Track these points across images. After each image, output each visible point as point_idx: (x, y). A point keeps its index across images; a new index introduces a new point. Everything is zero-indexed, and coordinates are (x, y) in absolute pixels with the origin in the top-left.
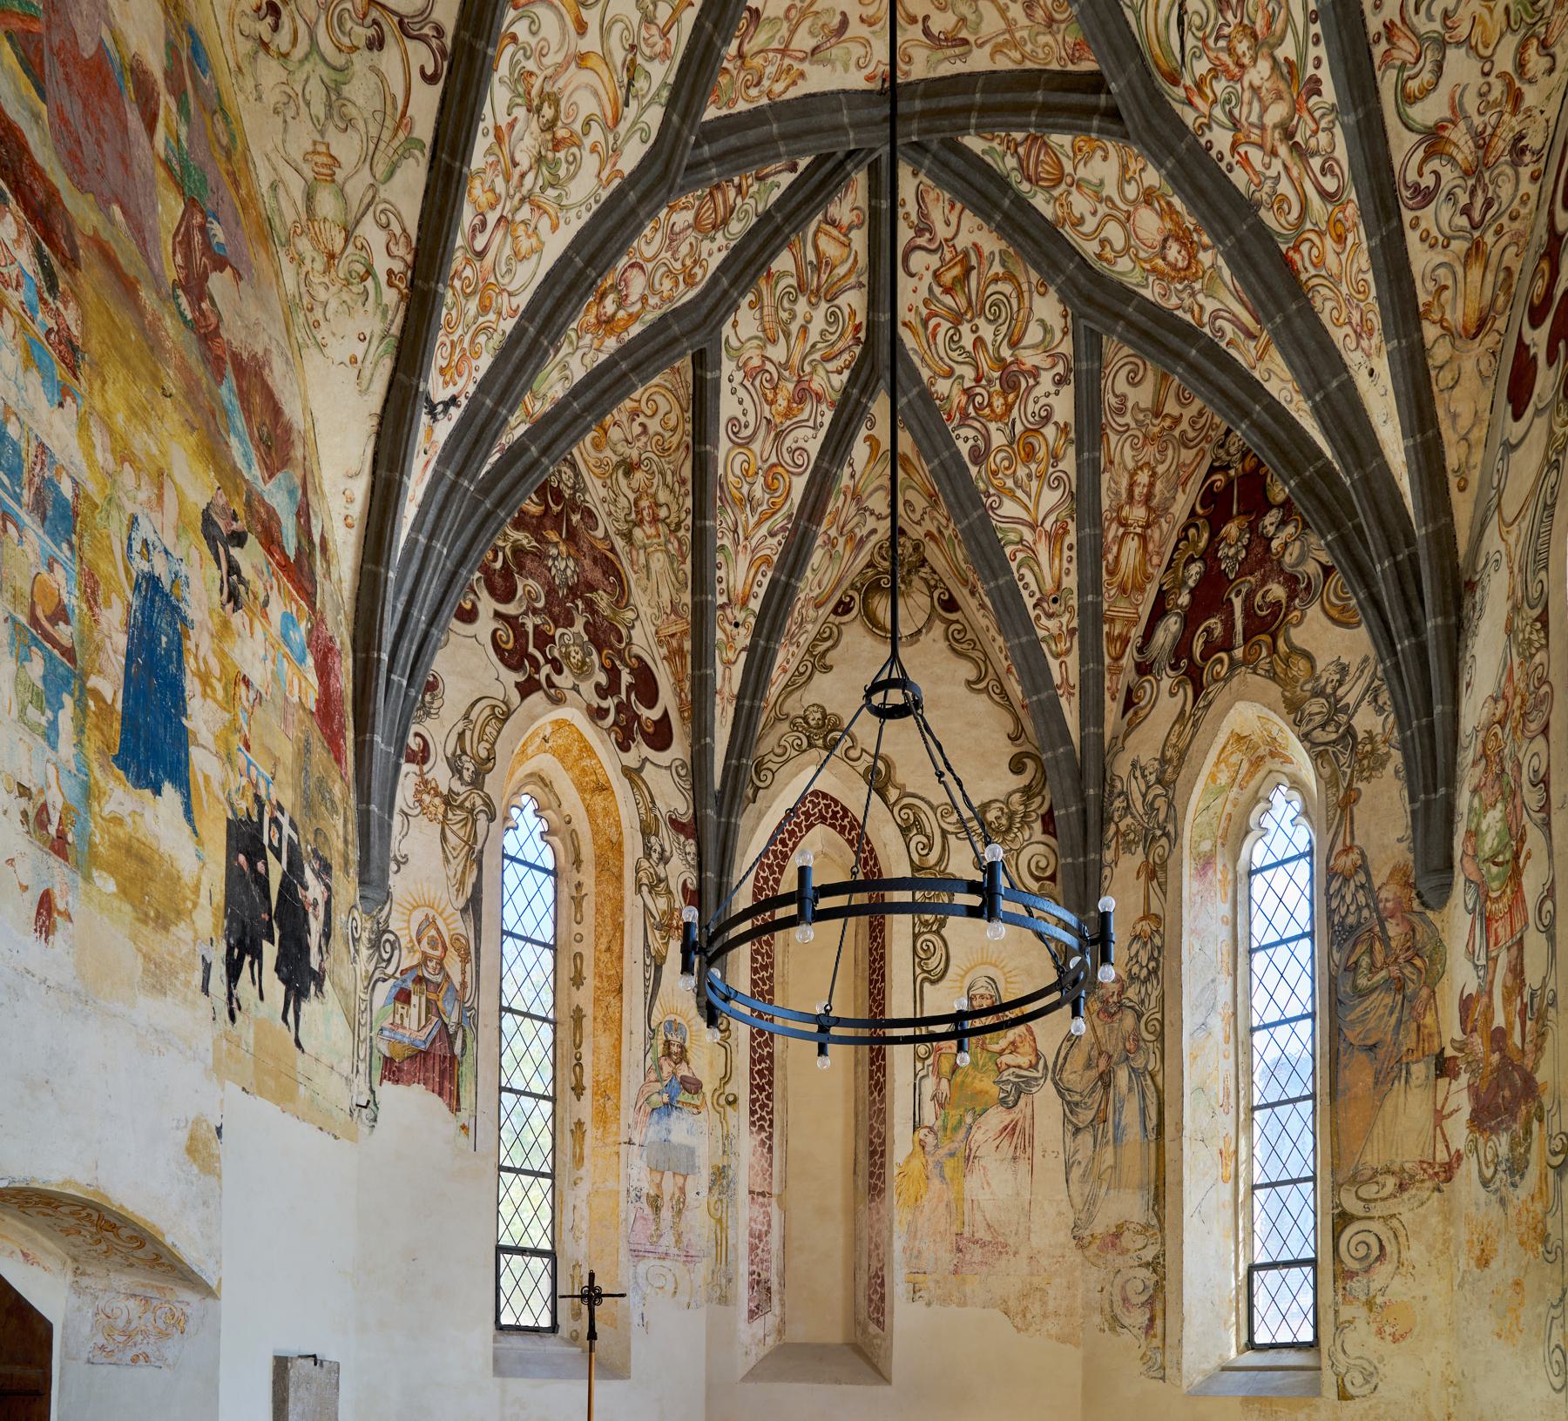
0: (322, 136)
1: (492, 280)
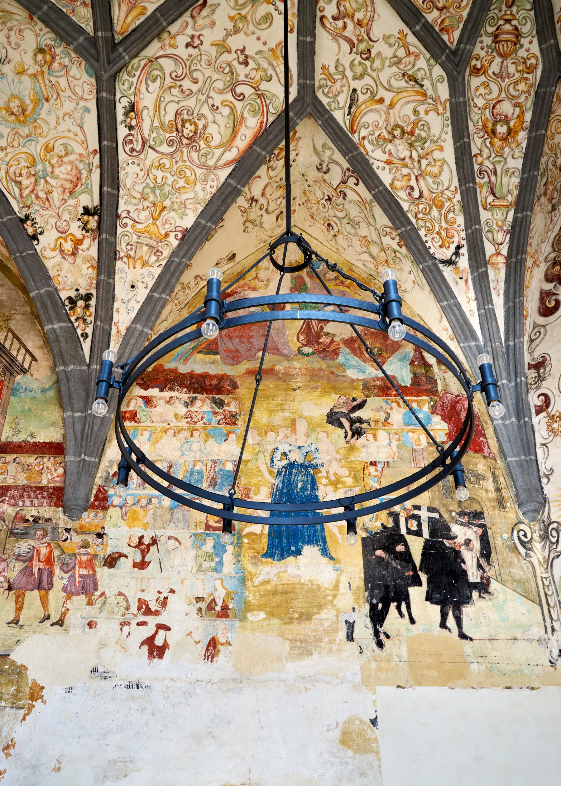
0: (358, 235)
1: (434, 195)
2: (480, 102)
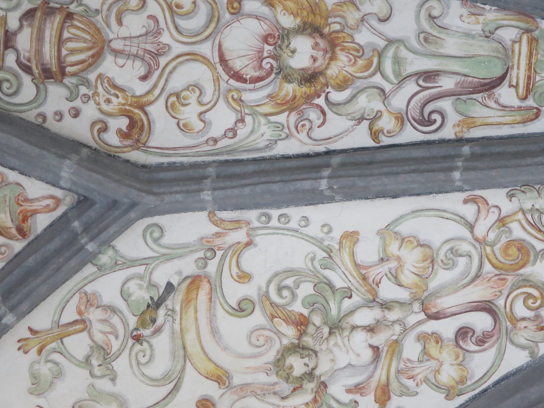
1: (488, 267)
2: (222, 118)
